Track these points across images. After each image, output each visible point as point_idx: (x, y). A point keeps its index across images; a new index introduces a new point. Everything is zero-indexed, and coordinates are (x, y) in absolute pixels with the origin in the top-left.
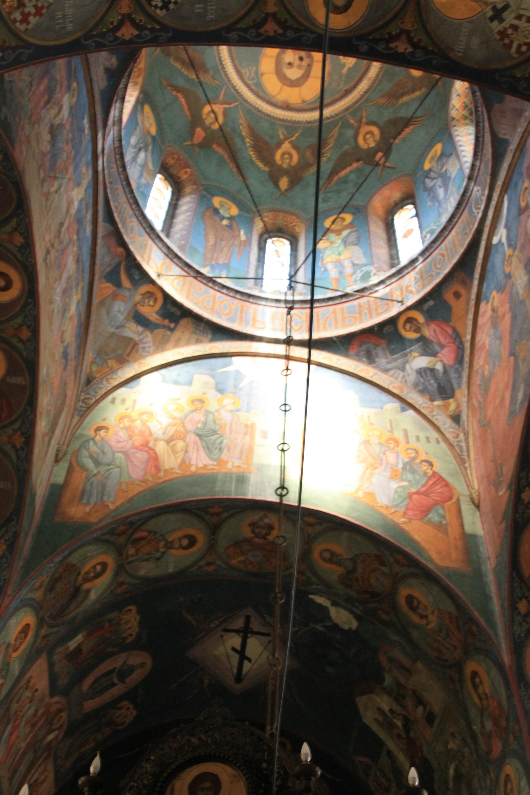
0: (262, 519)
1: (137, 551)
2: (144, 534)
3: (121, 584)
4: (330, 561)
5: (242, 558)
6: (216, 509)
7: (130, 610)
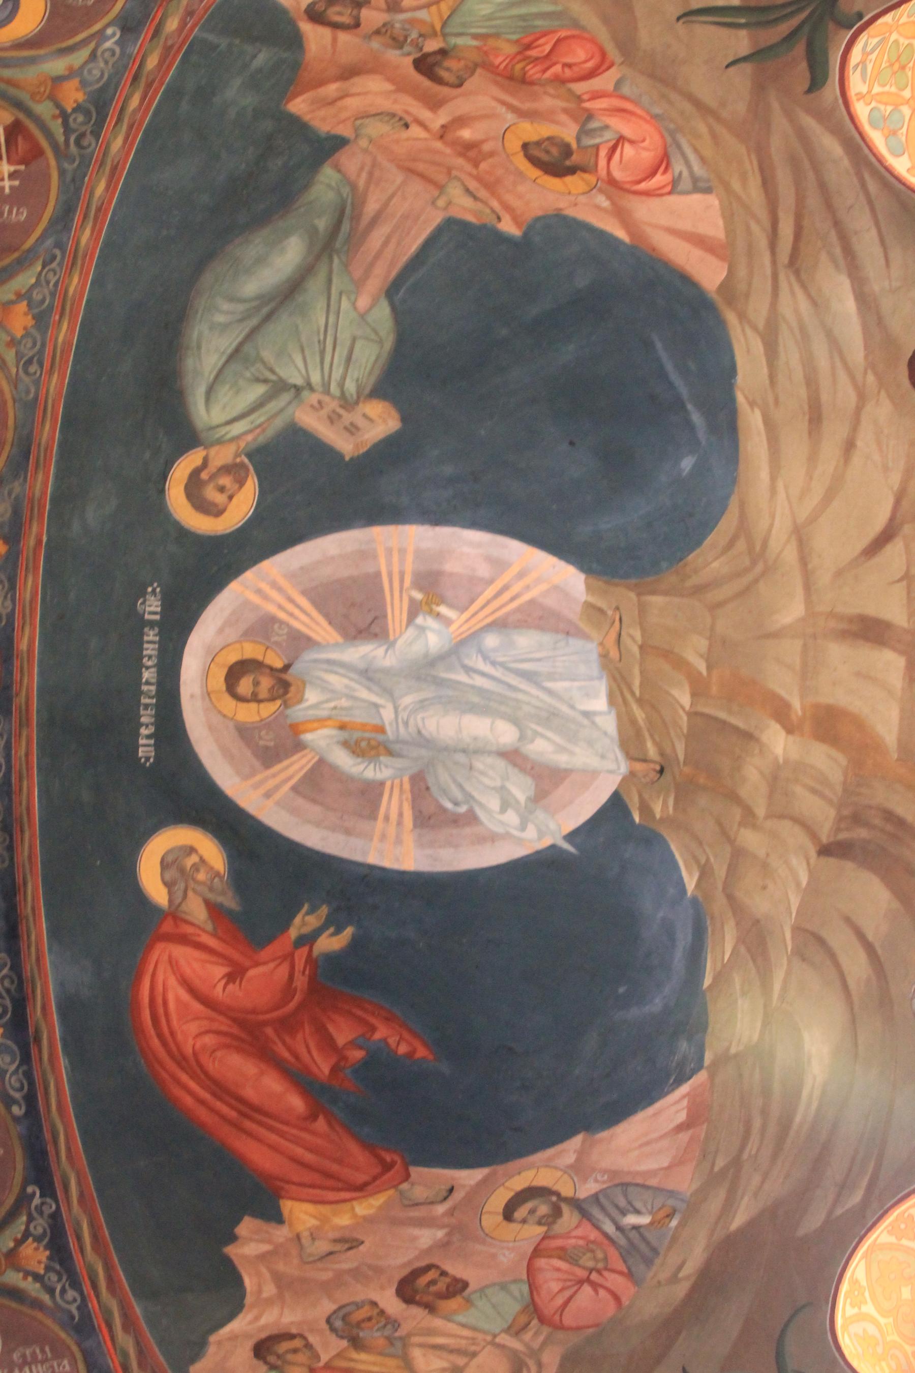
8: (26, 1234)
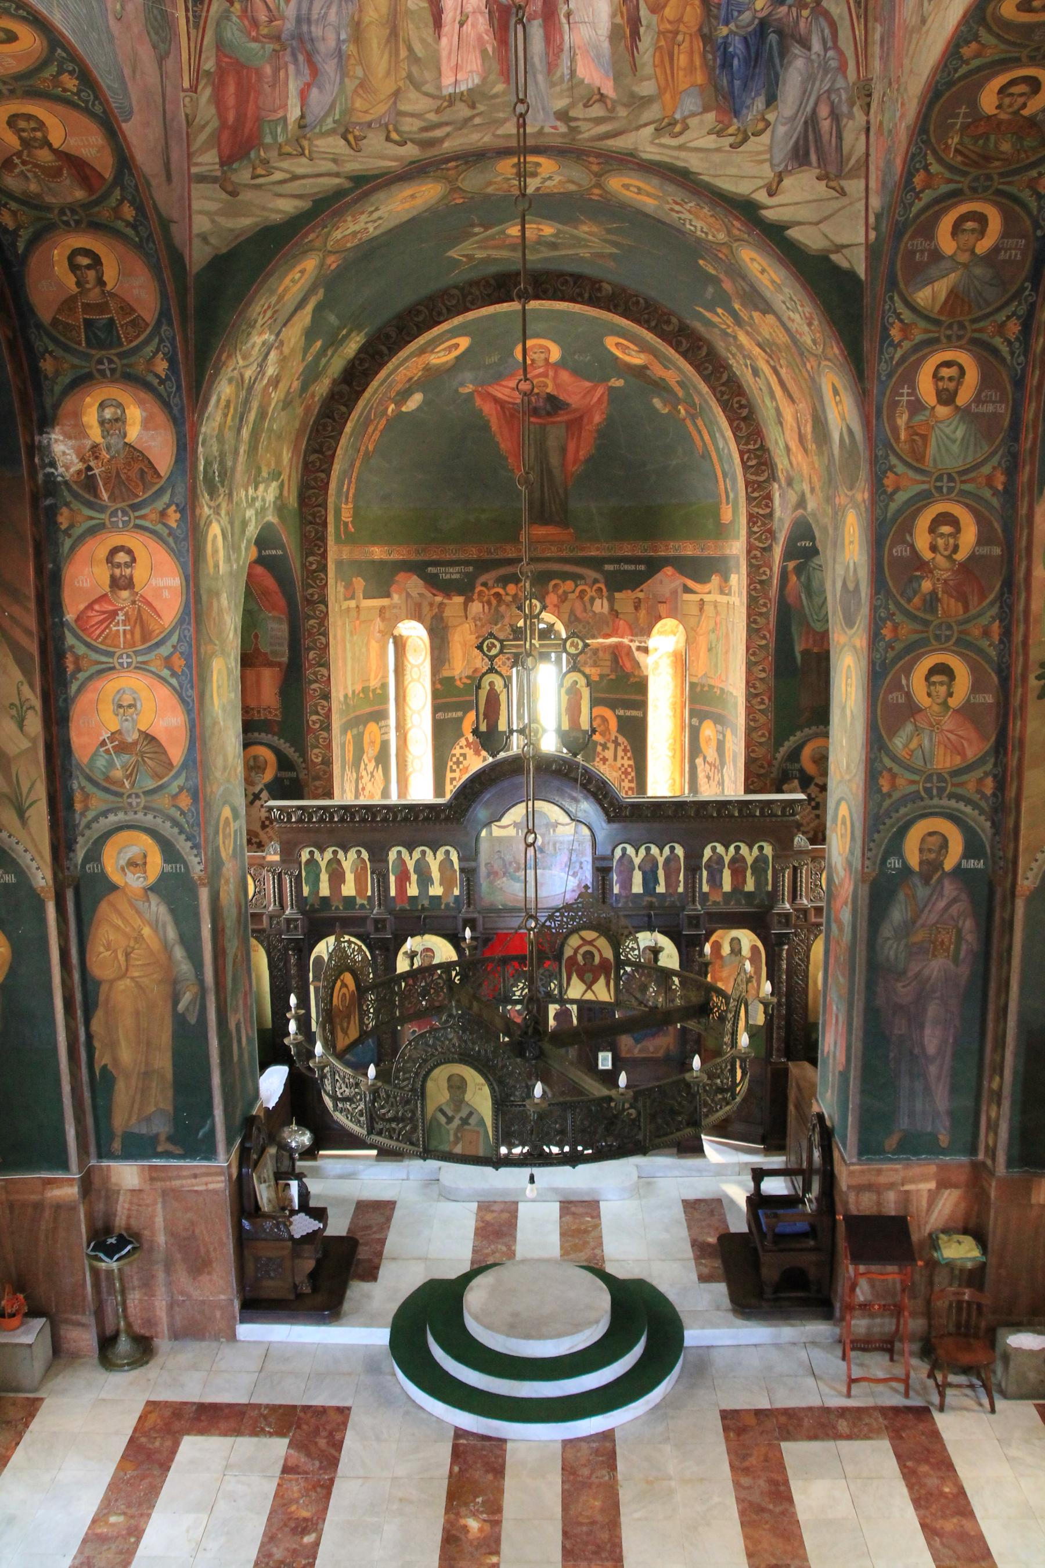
8: (1014, 314)
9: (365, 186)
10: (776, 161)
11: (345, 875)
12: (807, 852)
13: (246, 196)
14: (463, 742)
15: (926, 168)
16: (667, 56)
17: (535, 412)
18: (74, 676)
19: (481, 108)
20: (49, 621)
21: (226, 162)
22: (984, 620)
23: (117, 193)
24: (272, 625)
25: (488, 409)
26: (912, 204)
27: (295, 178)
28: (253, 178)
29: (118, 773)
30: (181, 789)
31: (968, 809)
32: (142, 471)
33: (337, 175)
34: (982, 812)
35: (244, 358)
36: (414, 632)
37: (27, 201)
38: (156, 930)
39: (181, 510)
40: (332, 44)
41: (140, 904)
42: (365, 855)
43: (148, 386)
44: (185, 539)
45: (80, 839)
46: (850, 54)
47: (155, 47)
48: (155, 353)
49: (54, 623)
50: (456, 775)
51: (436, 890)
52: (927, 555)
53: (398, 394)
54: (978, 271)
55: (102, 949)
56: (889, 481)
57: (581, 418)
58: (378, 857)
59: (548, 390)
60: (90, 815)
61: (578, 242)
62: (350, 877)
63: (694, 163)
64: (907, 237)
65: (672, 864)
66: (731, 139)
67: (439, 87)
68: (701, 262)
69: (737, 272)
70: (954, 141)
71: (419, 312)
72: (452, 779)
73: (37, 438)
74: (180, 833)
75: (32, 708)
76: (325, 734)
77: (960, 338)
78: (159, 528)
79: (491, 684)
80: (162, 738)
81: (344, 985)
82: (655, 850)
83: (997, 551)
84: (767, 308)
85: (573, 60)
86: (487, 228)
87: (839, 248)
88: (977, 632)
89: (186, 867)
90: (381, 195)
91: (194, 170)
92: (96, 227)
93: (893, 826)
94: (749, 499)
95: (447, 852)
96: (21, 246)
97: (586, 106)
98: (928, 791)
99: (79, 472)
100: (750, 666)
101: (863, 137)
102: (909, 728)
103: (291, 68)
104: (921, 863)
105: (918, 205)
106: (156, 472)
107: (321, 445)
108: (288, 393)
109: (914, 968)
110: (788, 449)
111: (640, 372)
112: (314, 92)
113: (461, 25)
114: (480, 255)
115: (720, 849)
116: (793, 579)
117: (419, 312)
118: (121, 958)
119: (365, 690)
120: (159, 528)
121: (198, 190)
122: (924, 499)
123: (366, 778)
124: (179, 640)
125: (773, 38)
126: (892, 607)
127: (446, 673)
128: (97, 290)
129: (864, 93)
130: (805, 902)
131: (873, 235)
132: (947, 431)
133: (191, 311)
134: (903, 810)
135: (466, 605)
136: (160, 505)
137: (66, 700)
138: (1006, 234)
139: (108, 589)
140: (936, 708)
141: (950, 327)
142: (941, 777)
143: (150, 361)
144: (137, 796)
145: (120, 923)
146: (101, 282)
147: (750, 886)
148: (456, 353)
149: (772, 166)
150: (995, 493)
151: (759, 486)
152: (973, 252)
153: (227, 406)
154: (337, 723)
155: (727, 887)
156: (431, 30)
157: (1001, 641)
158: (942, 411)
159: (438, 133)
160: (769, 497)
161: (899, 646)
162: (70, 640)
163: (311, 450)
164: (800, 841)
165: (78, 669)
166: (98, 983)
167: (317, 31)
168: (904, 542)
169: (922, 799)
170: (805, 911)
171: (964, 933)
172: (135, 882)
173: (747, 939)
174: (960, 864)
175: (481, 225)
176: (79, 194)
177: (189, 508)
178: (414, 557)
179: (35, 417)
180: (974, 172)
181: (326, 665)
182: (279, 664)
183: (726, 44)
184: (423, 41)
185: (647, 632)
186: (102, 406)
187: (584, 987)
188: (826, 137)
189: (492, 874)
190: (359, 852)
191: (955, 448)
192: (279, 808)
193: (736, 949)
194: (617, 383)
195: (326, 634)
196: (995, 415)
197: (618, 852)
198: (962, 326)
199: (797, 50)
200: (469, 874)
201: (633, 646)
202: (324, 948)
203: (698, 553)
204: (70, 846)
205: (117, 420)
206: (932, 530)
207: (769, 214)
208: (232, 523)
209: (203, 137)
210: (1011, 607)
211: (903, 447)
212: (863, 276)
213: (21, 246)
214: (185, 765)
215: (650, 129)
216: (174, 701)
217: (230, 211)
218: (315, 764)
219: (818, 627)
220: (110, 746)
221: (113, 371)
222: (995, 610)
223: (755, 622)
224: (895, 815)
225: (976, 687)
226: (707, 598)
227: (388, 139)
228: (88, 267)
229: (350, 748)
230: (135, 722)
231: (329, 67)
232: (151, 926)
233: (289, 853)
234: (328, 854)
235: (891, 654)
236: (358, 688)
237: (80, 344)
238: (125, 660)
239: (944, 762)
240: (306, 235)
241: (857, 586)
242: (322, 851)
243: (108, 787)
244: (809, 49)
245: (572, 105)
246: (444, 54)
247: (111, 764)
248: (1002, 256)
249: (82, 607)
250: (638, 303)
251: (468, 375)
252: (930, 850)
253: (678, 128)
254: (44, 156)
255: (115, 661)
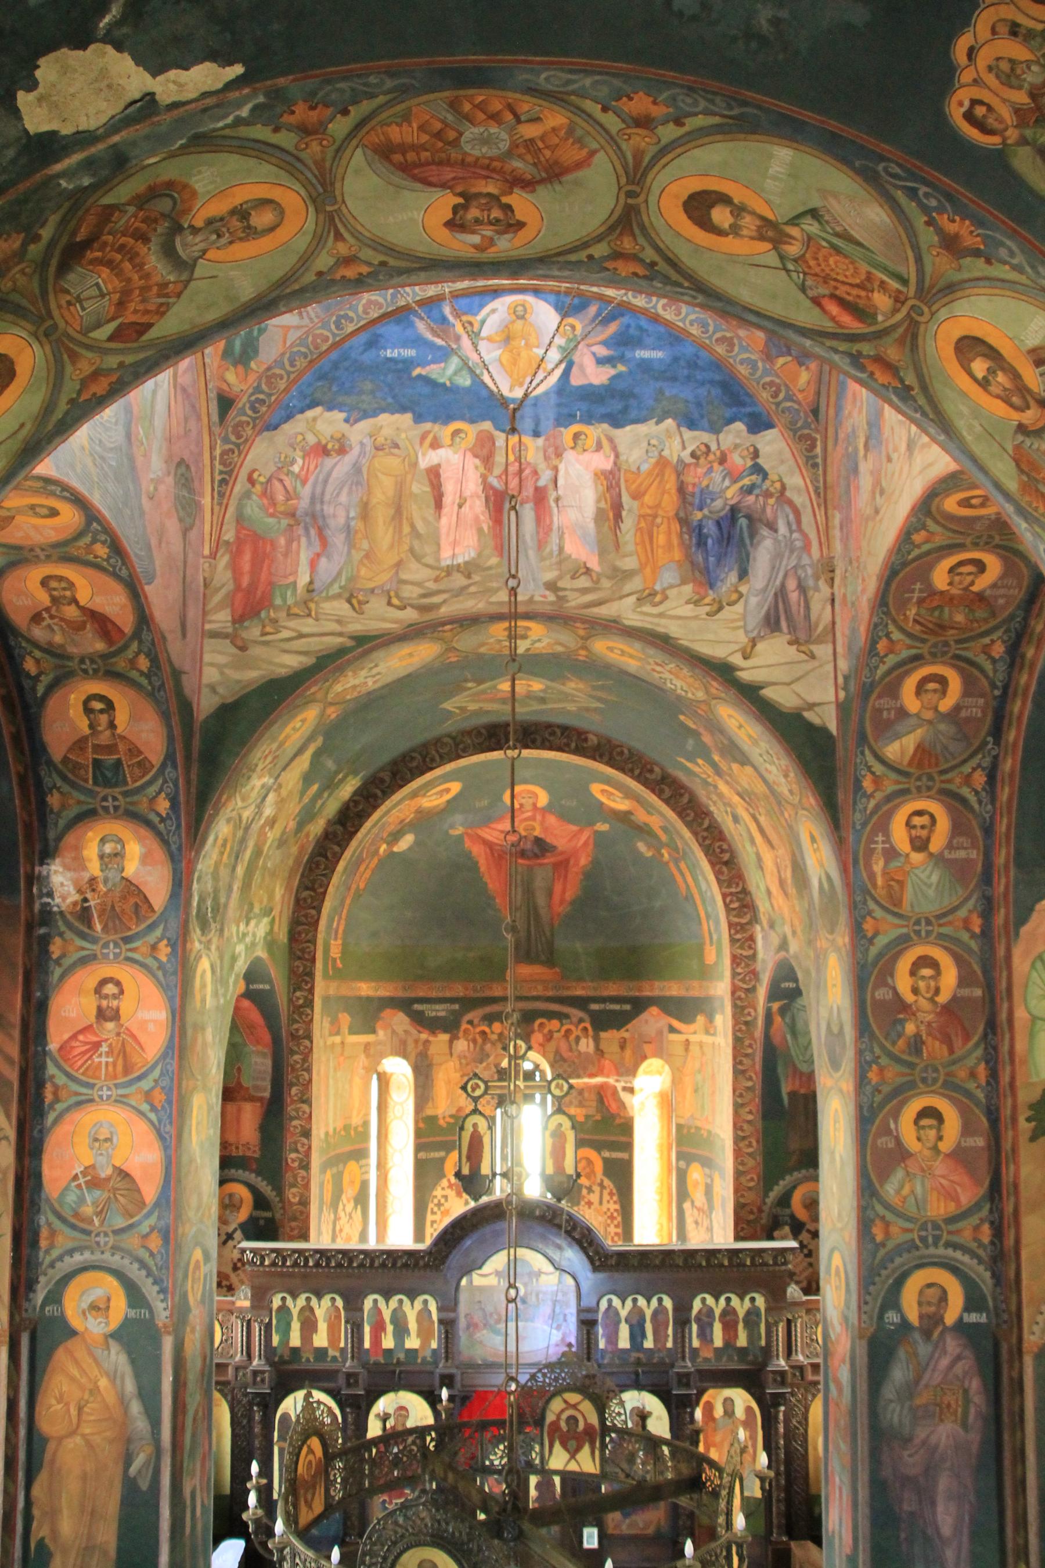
0: (491, 242)
1: (866, 284)
2: (834, 309)
3: (950, 244)
4: (242, 213)
5: (530, 131)
6: (625, 269)
7: (969, 116)
8: (979, 766)
9: (367, 644)
10: (750, 627)
11: (318, 1324)
12: (802, 1303)
13: (256, 651)
14: (444, 1183)
15: (888, 635)
16: (647, 535)
17: (523, 854)
18: (51, 1106)
19: (476, 578)
20: (32, 1048)
21: (238, 620)
22: (971, 1062)
23: (135, 646)
24: (256, 1059)
25: (478, 851)
26: (876, 668)
27: (301, 636)
28: (264, 634)
29: (88, 1210)
30: (152, 1229)
31: (966, 1259)
32: (136, 905)
33: (341, 634)
34: (980, 1261)
35: (243, 800)
36: (399, 1069)
37: (50, 650)
38: (113, 1379)
39: (172, 945)
40: (342, 520)
41: (98, 1352)
42: (340, 1303)
43: (148, 824)
44: (175, 973)
45: (42, 1279)
46: (813, 535)
47: (181, 520)
48: (159, 793)
49: (36, 1052)
50: (437, 1217)
51: (412, 1342)
52: (909, 998)
53: (391, 834)
54: (942, 727)
55: (53, 1402)
56: (868, 926)
57: (567, 861)
58: (353, 1305)
59: (536, 833)
60: (55, 1253)
61: (566, 697)
62: (322, 1326)
63: (674, 629)
64: (874, 696)
65: (660, 1317)
66: (708, 608)
67: (438, 560)
68: (682, 717)
69: (716, 727)
70: (912, 612)
71: (413, 758)
72: (433, 1222)
73: (37, 869)
74: (148, 1275)
75: (6, 1138)
76: (303, 1173)
77: (929, 788)
78: (150, 961)
79: (475, 1125)
80: (136, 1174)
81: (311, 1451)
82: (642, 1302)
83: (978, 992)
84: (744, 760)
85: (561, 538)
86: (480, 682)
87: (811, 706)
88: (963, 1074)
89: (151, 1312)
90: (380, 654)
91: (207, 627)
92: (113, 675)
93: (888, 1277)
94: (733, 941)
95: (426, 1302)
96: (40, 689)
97: (573, 578)
98: (923, 1239)
99: (75, 904)
100: (737, 1107)
101: (829, 607)
102: (900, 1174)
103: (303, 540)
104: (921, 1317)
105: (882, 669)
106: (150, 906)
107: (313, 882)
108: (284, 833)
109: (921, 1434)
110: (769, 893)
111: (624, 818)
112: (323, 561)
113: (460, 506)
114: (473, 707)
115: (710, 1300)
116: (778, 1019)
117: (413, 758)
118: (74, 1412)
119: (346, 1128)
120: (150, 961)
121: (209, 644)
122: (902, 943)
123: (344, 1219)
124: (162, 1074)
125: (743, 522)
126: (877, 1050)
127: (429, 1112)
128: (108, 733)
129: (829, 570)
130: (801, 1358)
131: (842, 694)
132: (923, 876)
133: (195, 755)
134: (898, 1261)
135: (451, 1042)
136: (151, 938)
137: (41, 1131)
138: (966, 693)
139: (93, 1019)
140: (927, 1153)
141: (919, 779)
142: (936, 1226)
143: (152, 800)
144: (106, 1235)
145: (76, 1373)
146: (112, 725)
147: (742, 1341)
148: (448, 797)
149: (746, 632)
150: (973, 936)
151: (742, 928)
152: (936, 709)
153: (224, 845)
154: (316, 1161)
155: (718, 1342)
156: (432, 510)
157: (988, 1083)
158: (917, 857)
159: (436, 600)
160: (752, 939)
161: (886, 1089)
162: (51, 1069)
163: (303, 886)
164: (793, 1291)
165: (57, 1099)
166: (45, 1440)
167: (328, 510)
168: (885, 984)
169: (917, 1248)
170: (801, 1368)
171: (972, 1392)
172: (95, 1327)
173: (741, 1399)
174: (961, 1319)
175: (473, 680)
176: (100, 646)
177: (180, 943)
178: (401, 994)
179: (38, 847)
180: (933, 640)
181: (308, 1102)
182: (261, 1099)
183: (700, 527)
184: (424, 519)
185: (633, 1072)
186: (103, 841)
187: (567, 1456)
188: (794, 608)
189: (472, 1326)
190: (333, 1300)
191: (931, 892)
192: (252, 1250)
193: (729, 1412)
194: (603, 827)
195: (309, 1070)
196: (968, 861)
197: (604, 1304)
198: (931, 778)
199: (765, 532)
200: (448, 1325)
201: (619, 1086)
202: (292, 1405)
203: (683, 993)
204: (31, 1286)
205: (116, 855)
206: (913, 973)
207: (745, 676)
208: (221, 958)
209: (217, 598)
210: (995, 1048)
211: (880, 893)
212: (834, 732)
213: (40, 689)
214: (157, 1204)
215: (633, 599)
216: (152, 1137)
217: (238, 665)
218: (291, 1203)
219: (804, 1068)
220: (82, 1181)
221: (116, 808)
222: (979, 1052)
223: (741, 1063)
224: (891, 1266)
225: (967, 1130)
226: (693, 1038)
227: (389, 604)
228: (102, 711)
229: (329, 1188)
230: (109, 1157)
231: (338, 540)
232: (108, 1375)
233: (260, 1298)
234: (301, 1301)
235: (878, 1098)
236: (340, 1125)
237: (86, 781)
238: (105, 1093)
239: (938, 1209)
240: (309, 688)
241: (841, 1028)
242: (295, 1297)
243: (77, 1224)
244: (776, 531)
245: (560, 577)
246: (443, 531)
247: (82, 1200)
248: (964, 714)
249: (66, 1036)
250: (622, 753)
251: (458, 818)
252: (929, 1303)
253: (658, 598)
254: (71, 612)
255: (95, 1094)
